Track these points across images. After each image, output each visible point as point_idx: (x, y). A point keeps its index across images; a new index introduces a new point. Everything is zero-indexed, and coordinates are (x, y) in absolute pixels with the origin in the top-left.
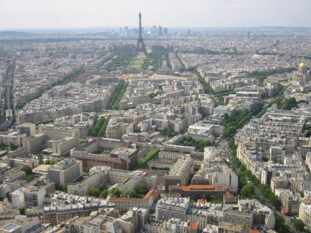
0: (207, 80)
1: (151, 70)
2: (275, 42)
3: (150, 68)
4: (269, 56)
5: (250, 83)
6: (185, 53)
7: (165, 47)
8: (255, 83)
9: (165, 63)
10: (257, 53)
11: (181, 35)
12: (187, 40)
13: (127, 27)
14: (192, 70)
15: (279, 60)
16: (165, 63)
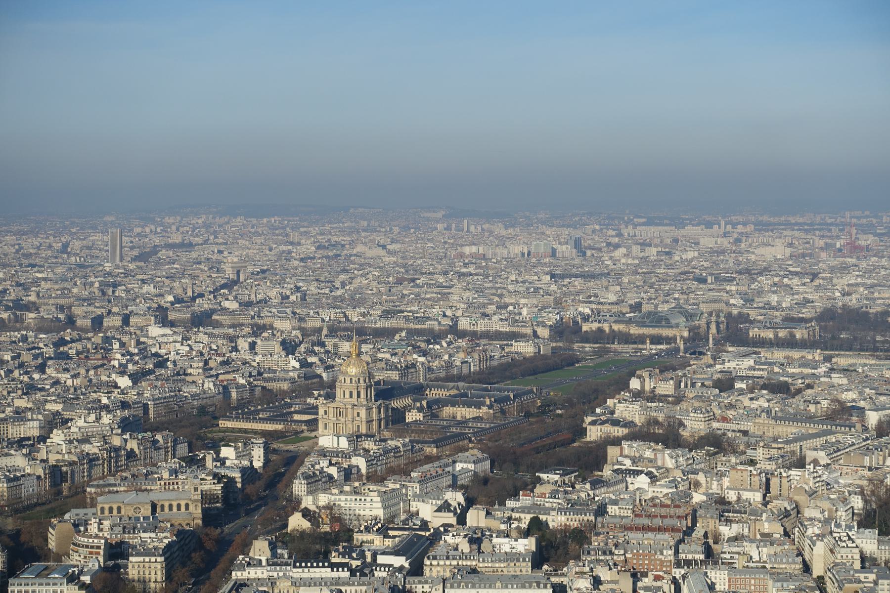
4: (210, 330)
10: (163, 320)
15: (252, 346)
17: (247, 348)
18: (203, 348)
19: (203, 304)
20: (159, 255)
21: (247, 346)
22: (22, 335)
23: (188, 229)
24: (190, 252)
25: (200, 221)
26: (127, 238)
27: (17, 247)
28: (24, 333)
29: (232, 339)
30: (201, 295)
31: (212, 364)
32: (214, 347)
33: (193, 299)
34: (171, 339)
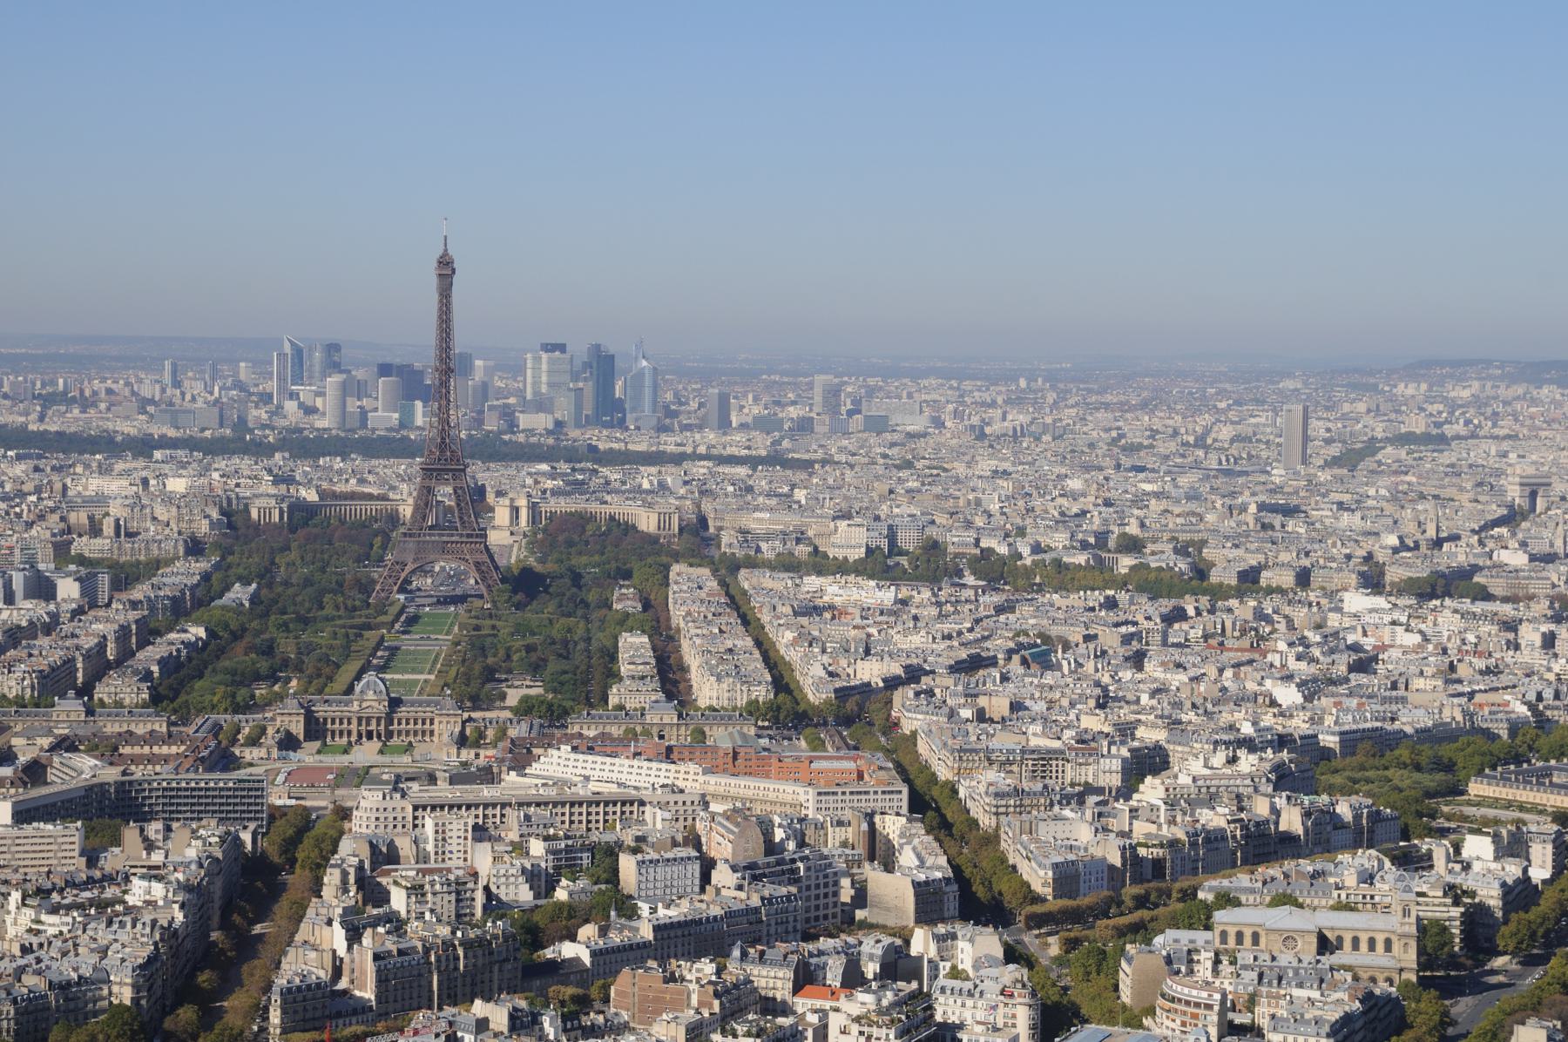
0: (977, 793)
1: (526, 708)
2: (1515, 494)
3: (513, 697)
5: (1326, 836)
6: (788, 565)
7: (647, 522)
8: (1360, 836)
9: (634, 647)
10: (1373, 581)
11: (764, 424)
12: (807, 465)
13: (332, 348)
14: (856, 714)
15: (1549, 641)
16: (634, 647)
17: (1538, 642)
18: (1449, 639)
19: (1457, 555)
20: (1379, 456)
21: (1538, 640)
22: (1107, 598)
23: (1441, 407)
24: (1441, 451)
25: (1466, 394)
26: (1321, 423)
27: (1114, 434)
28: (1110, 593)
29: (1511, 626)
30: (1455, 538)
31: (1463, 671)
32: (1471, 638)
33: (1438, 543)
34: (1387, 619)
